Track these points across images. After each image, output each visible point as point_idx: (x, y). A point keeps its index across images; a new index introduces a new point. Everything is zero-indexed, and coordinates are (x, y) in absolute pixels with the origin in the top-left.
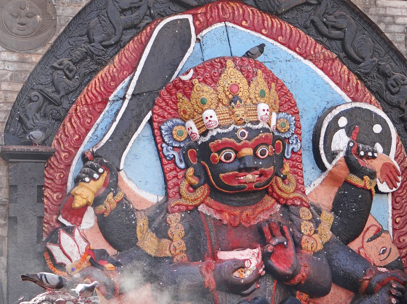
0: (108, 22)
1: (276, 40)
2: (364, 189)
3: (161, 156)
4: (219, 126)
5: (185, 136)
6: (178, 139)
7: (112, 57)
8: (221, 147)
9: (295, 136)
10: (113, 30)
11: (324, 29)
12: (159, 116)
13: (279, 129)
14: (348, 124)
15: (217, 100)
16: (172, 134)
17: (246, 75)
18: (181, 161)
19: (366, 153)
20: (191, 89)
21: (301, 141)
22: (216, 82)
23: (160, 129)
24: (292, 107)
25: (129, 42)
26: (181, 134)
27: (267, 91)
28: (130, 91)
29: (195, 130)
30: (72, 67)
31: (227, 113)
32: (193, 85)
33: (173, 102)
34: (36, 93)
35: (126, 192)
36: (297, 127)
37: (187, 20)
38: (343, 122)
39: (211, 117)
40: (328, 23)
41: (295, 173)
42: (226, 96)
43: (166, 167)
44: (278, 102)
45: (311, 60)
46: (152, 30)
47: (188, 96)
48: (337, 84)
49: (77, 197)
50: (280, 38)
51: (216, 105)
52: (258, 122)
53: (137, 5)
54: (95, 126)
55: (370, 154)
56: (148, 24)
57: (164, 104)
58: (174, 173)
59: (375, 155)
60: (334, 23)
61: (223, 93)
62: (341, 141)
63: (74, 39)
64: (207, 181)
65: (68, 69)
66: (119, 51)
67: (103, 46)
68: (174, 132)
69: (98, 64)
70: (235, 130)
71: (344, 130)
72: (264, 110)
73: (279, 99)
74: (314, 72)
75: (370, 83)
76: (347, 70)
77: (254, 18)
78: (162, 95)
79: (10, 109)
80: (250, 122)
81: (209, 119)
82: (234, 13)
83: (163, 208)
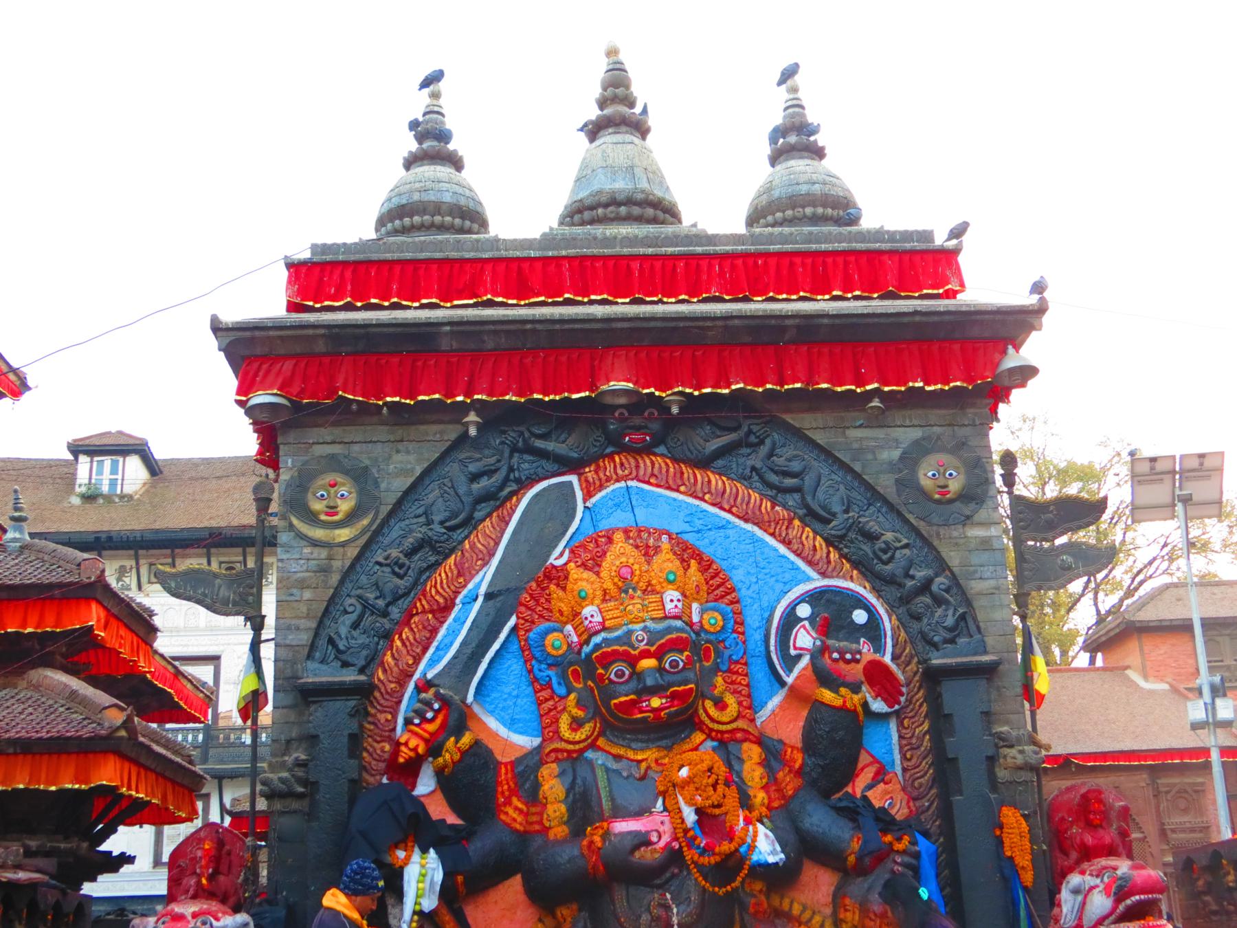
0: (451, 491)
1: (702, 499)
2: (843, 708)
3: (535, 680)
4: (604, 629)
5: (565, 647)
6: (554, 652)
7: (462, 542)
9: (735, 635)
10: (460, 505)
11: (773, 478)
13: (706, 627)
14: (813, 613)
18: (560, 684)
19: (842, 653)
20: (566, 578)
21: (744, 642)
23: (526, 640)
25: (484, 520)
28: (483, 590)
29: (575, 639)
30: (403, 559)
32: (568, 573)
34: (353, 601)
35: (482, 736)
36: (736, 622)
37: (571, 483)
38: (804, 611)
41: (735, 692)
42: (615, 584)
44: (705, 588)
46: (519, 501)
47: (564, 589)
48: (798, 555)
49: (403, 748)
50: (707, 497)
52: (666, 617)
54: (435, 644)
55: (848, 656)
56: (514, 493)
57: (532, 603)
58: (551, 703)
59: (858, 657)
62: (804, 639)
63: (407, 522)
64: (597, 713)
65: (396, 563)
66: (470, 533)
68: (547, 642)
69: (438, 553)
70: (630, 632)
71: (806, 623)
74: (762, 540)
75: (846, 550)
76: (811, 535)
77: (667, 471)
78: (529, 593)
79: (314, 625)
80: (653, 619)
82: (637, 467)
83: (538, 757)
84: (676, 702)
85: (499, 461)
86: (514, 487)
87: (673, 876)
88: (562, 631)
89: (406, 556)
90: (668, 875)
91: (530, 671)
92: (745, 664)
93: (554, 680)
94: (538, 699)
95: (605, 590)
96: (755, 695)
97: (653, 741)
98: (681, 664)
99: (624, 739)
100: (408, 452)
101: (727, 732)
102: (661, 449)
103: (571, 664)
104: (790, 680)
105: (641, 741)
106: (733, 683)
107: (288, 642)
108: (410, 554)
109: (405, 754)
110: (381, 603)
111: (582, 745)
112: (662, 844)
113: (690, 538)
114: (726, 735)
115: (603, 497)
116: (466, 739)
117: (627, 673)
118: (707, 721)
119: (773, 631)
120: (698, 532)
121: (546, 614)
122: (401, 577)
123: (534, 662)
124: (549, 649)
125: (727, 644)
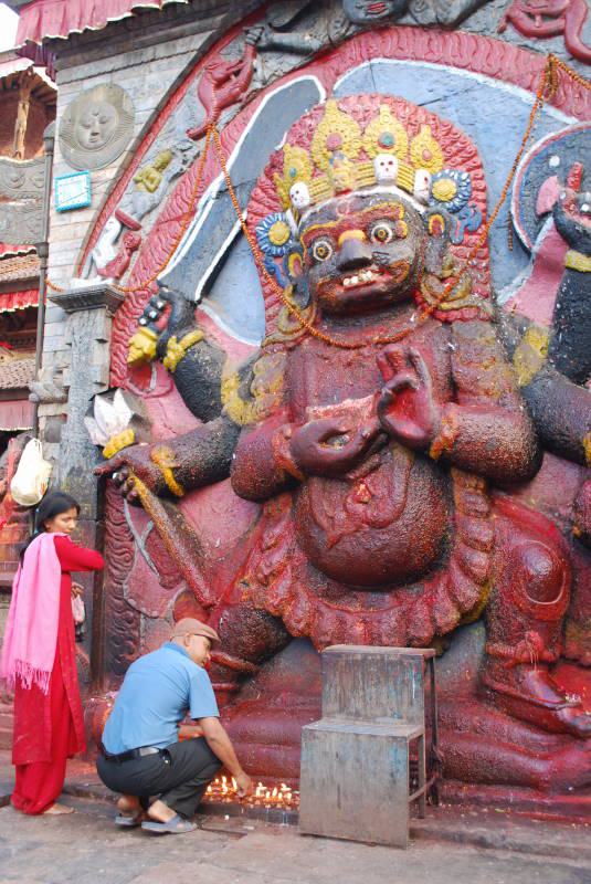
6: (277, 243)
8: (312, 238)
12: (255, 214)
22: (310, 139)
24: (469, 159)
30: (155, 174)
33: (275, 190)
40: (532, 11)
46: (263, 97)
49: (132, 349)
53: (235, 69)
57: (262, 194)
60: (544, 9)
65: (147, 178)
67: (190, 136)
72: (382, 164)
73: (444, 150)
81: (296, 196)
85: (241, 62)
86: (258, 85)
89: (157, 169)
95: (315, 164)
100: (159, 67)
101: (453, 309)
102: (408, 19)
103: (291, 252)
104: (535, 249)
107: (59, 263)
108: (162, 167)
109: (134, 354)
110: (134, 218)
111: (296, 335)
115: (346, 81)
116: (190, 337)
117: (330, 248)
121: (273, 203)
122: (150, 191)
124: (272, 239)
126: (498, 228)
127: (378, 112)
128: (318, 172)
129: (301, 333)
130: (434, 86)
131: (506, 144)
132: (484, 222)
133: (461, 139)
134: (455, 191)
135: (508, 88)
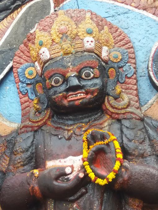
5: (35, 74)
6: (30, 78)
12: (18, 63)
13: (111, 59)
15: (51, 40)
16: (24, 74)
17: (75, 19)
18: (32, 93)
21: (135, 68)
22: (50, 28)
24: (127, 44)
25: (3, 19)
26: (30, 74)
27: (96, 29)
29: (39, 68)
31: (58, 48)
39: (44, 52)
43: (21, 100)
45: (144, 10)
46: (21, 9)
47: (34, 43)
51: (51, 44)
57: (22, 54)
58: (28, 103)
61: (55, 34)
68: (26, 73)
72: (88, 42)
74: (147, 17)
84: (89, 96)
87: (83, 195)
88: (34, 66)
90: (79, 194)
91: (18, 89)
92: (135, 79)
93: (29, 92)
94: (21, 102)
95: (53, 40)
96: (141, 96)
97: (78, 120)
98: (92, 75)
99: (63, 119)
103: (37, 82)
105: (71, 120)
106: (126, 89)
111: (40, 124)
112: (75, 174)
113: (108, 19)
114: (121, 115)
117: (60, 80)
118: (110, 109)
119: (151, 59)
120: (113, 16)
123: (20, 83)
124: (27, 76)
125: (124, 69)
126: (141, 76)
127: (85, 18)
128: (54, 43)
129: (42, 122)
130: (108, 10)
131: (144, 38)
132: (135, 73)
133: (123, 35)
134: (121, 57)
135: (145, 13)
